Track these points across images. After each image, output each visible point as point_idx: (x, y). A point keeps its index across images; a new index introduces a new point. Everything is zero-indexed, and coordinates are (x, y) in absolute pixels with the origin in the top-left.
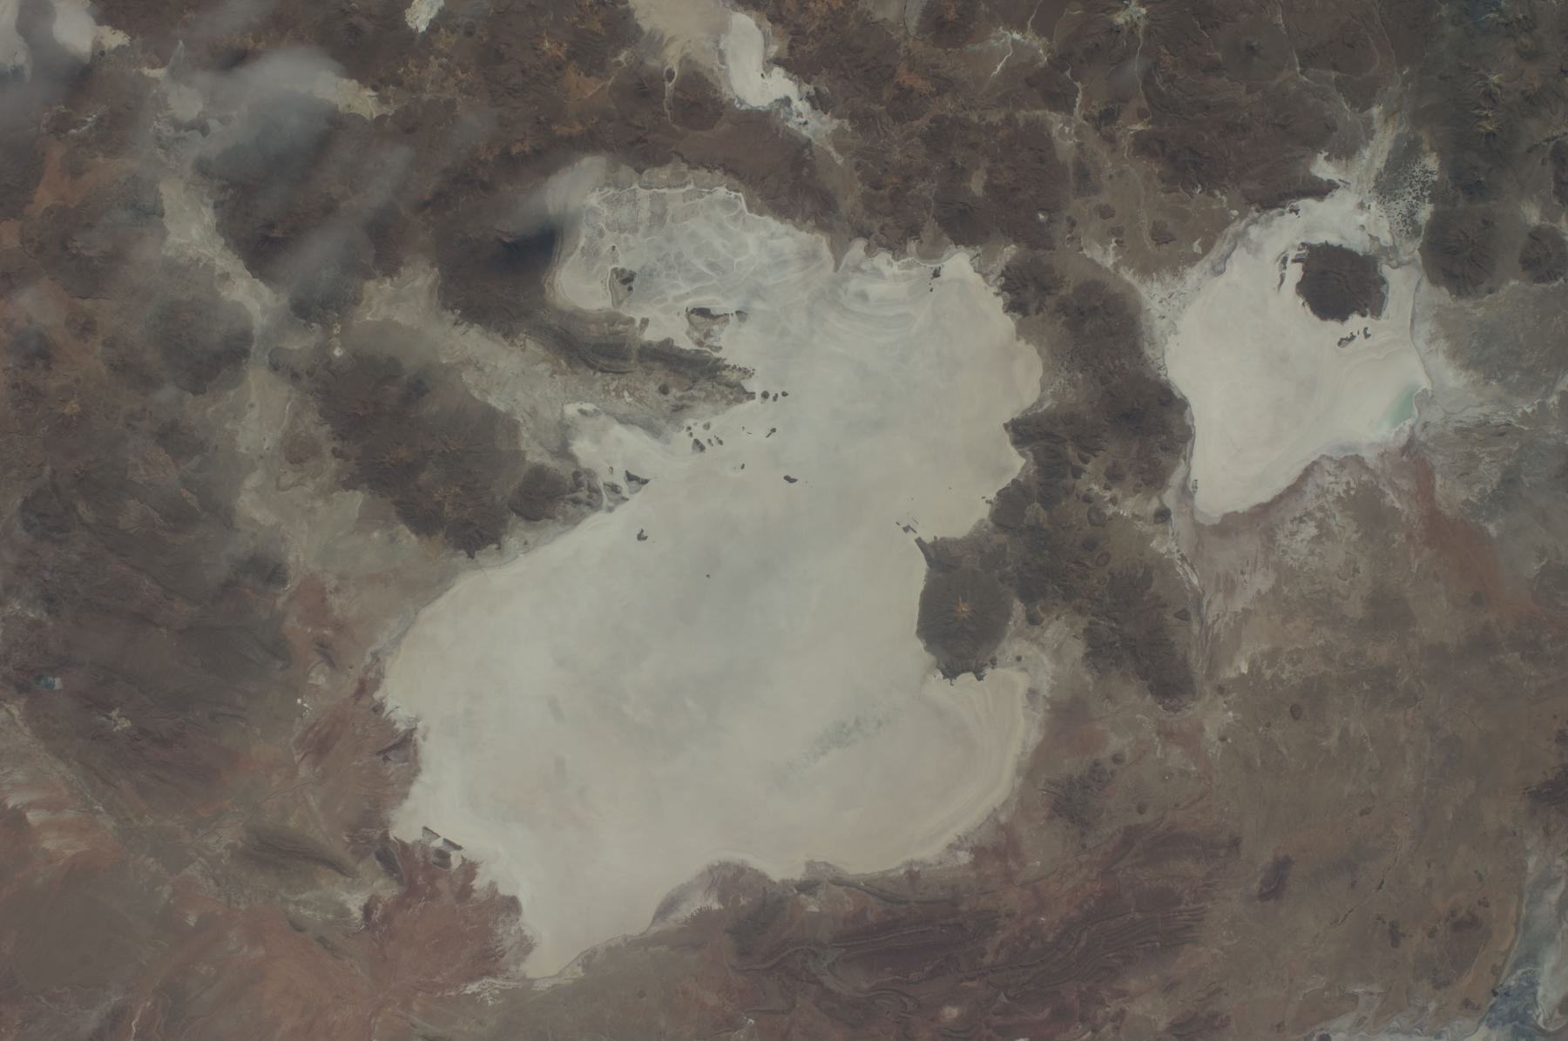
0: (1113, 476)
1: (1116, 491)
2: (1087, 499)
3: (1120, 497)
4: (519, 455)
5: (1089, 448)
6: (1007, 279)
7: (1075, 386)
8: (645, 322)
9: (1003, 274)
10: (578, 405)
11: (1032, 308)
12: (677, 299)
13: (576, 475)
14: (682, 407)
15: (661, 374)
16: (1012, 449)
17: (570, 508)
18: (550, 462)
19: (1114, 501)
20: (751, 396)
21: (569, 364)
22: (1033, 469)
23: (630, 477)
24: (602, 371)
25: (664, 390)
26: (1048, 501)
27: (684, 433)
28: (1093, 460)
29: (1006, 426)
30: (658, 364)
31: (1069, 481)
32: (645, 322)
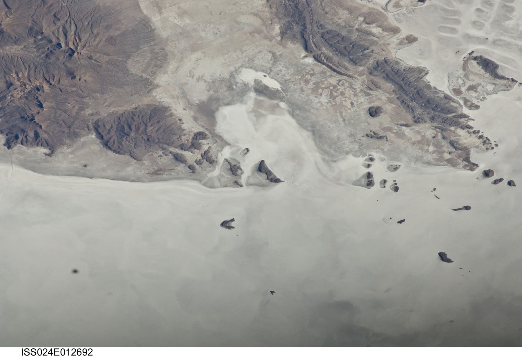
4: (148, 85)
8: (411, 40)
10: (260, 75)
12: (468, 38)
13: (199, 135)
14: (382, 137)
15: (384, 96)
17: (166, 160)
18: (179, 110)
20: (473, 166)
21: (283, 34)
23: (261, 167)
24: (317, 59)
25: (374, 112)
27: (362, 160)
30: (389, 86)
32: (411, 40)
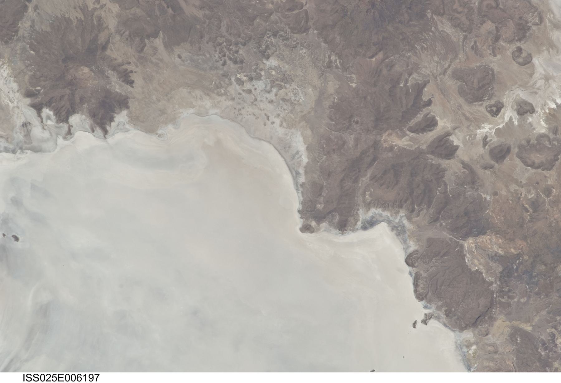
0: (480, 89)
1: (511, 97)
2: (500, 153)
3: (523, 95)
5: (405, 106)
6: (49, 104)
7: (286, 79)
9: (38, 108)
11: (117, 87)
16: (351, 237)
19: (525, 109)
22: (401, 217)
26: (472, 223)
28: (435, 110)
29: (306, 228)
31: (452, 168)
